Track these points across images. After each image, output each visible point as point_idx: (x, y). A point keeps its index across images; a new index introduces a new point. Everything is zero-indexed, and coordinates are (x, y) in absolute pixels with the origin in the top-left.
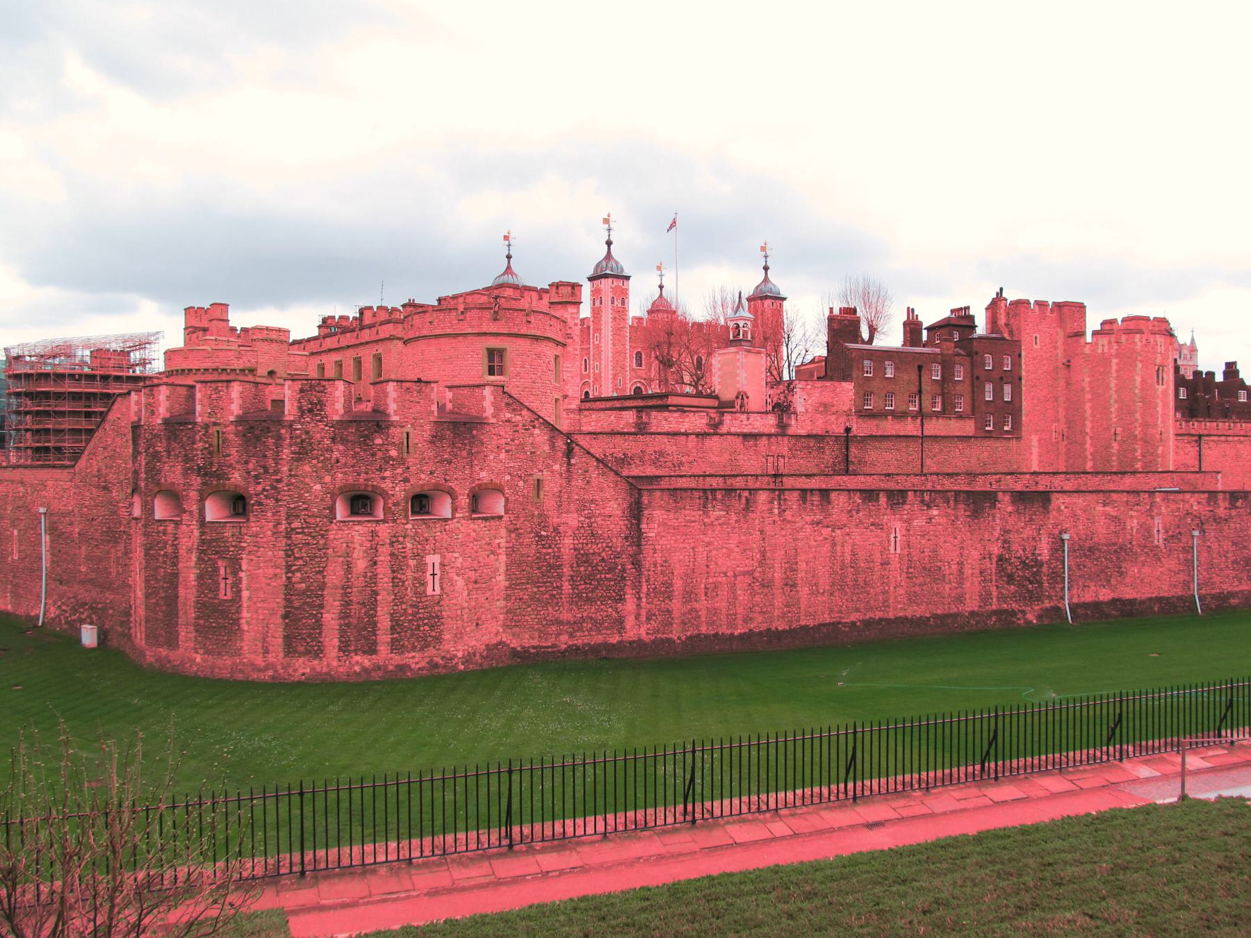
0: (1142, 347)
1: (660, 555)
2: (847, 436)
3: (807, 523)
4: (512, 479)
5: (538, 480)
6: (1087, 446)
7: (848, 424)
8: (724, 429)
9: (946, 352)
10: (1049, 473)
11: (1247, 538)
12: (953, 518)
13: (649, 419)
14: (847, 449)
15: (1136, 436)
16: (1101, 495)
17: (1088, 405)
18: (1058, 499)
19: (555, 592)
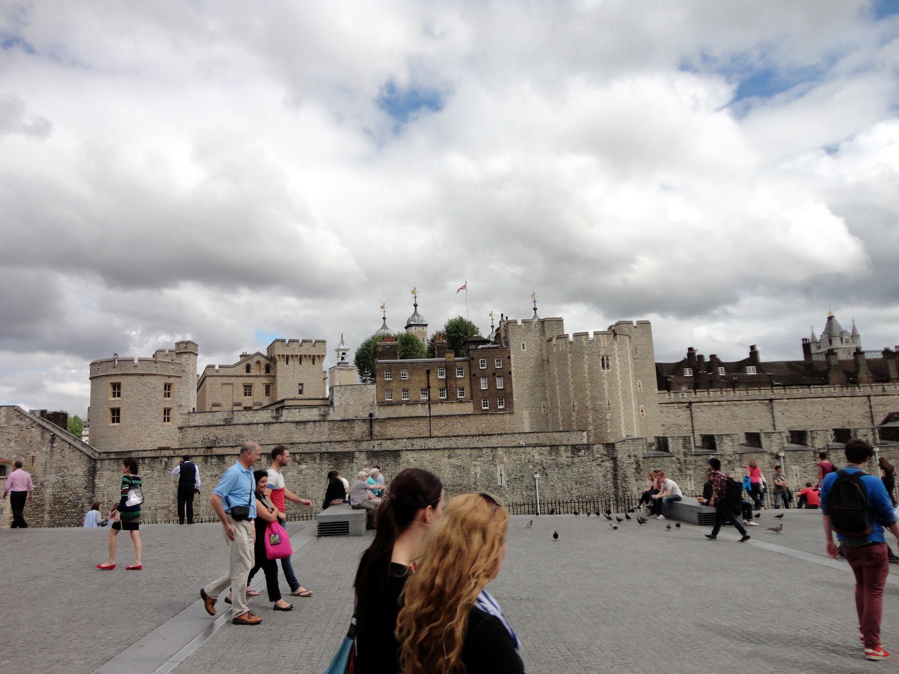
0: (587, 344)
1: (107, 497)
2: (371, 419)
3: (207, 476)
4: (18, 457)
5: (33, 457)
6: (559, 416)
7: (371, 411)
8: (283, 419)
9: (448, 360)
10: (423, 438)
11: (591, 478)
12: (319, 470)
13: (233, 415)
14: (371, 427)
15: (588, 407)
16: (446, 451)
17: (558, 387)
18: (407, 455)
19: (39, 520)
